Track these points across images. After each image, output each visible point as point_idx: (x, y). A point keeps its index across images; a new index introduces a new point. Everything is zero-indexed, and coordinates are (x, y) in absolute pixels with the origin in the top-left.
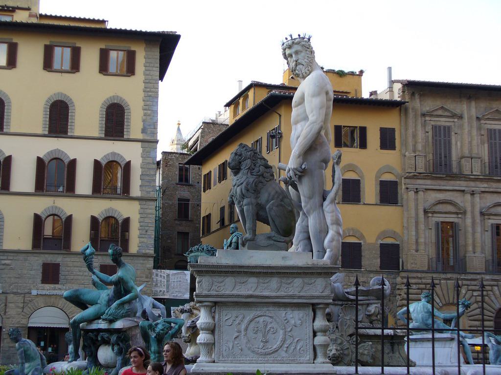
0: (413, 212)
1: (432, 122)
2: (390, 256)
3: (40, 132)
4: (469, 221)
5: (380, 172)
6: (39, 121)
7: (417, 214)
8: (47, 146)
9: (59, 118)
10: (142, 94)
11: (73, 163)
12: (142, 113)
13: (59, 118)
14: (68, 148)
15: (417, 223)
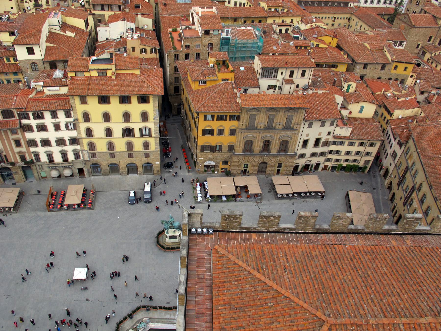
0: (239, 139)
1: (250, 113)
2: (231, 148)
3: (122, 122)
4: (257, 140)
5: (230, 127)
6: (121, 118)
7: (241, 138)
8: (125, 125)
9: (127, 117)
10: (153, 109)
11: (133, 129)
12: (153, 114)
13: (127, 117)
14: (130, 125)
15: (240, 142)
